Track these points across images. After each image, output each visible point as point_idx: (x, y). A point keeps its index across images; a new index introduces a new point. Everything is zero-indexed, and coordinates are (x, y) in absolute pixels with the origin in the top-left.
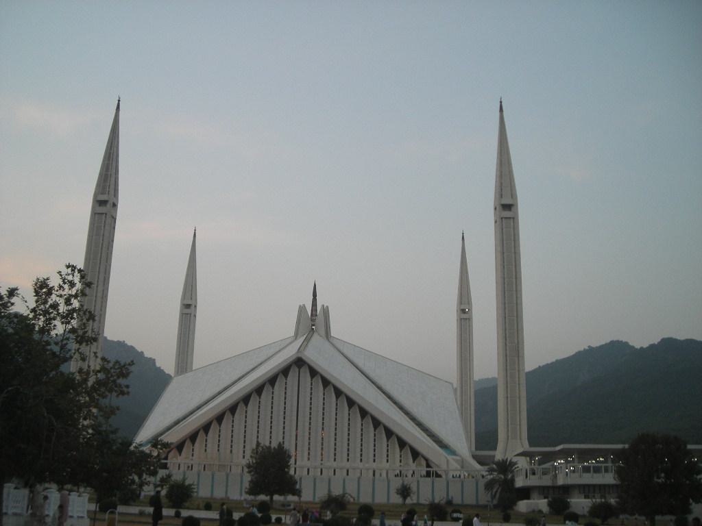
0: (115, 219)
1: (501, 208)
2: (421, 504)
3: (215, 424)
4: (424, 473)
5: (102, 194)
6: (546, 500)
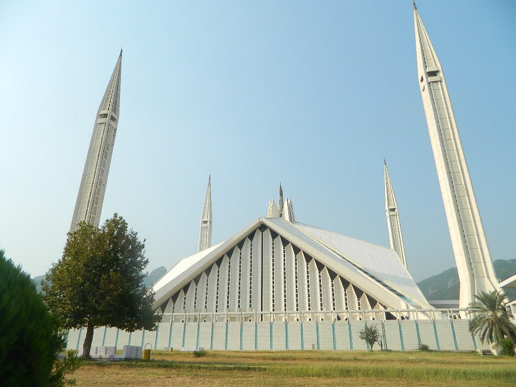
0: (116, 130)
1: (427, 76)
2: (390, 351)
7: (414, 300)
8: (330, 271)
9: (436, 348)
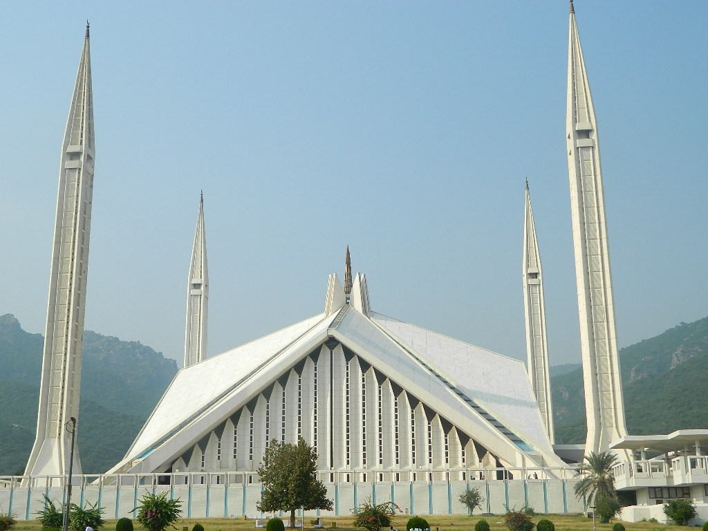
0: (93, 175)
1: (577, 135)
2: (493, 515)
3: (230, 424)
4: (494, 474)
5: (71, 144)
6: (661, 506)
7: (535, 448)
8: (426, 408)
9: (543, 512)
